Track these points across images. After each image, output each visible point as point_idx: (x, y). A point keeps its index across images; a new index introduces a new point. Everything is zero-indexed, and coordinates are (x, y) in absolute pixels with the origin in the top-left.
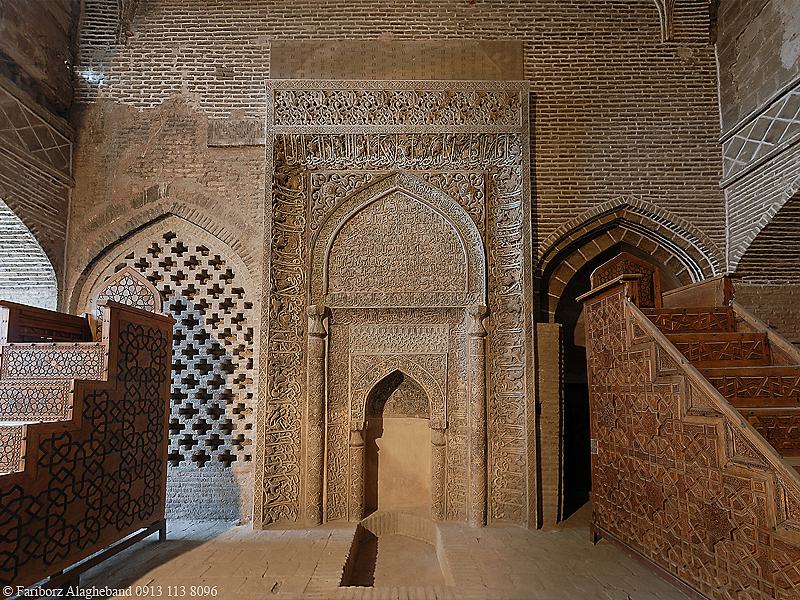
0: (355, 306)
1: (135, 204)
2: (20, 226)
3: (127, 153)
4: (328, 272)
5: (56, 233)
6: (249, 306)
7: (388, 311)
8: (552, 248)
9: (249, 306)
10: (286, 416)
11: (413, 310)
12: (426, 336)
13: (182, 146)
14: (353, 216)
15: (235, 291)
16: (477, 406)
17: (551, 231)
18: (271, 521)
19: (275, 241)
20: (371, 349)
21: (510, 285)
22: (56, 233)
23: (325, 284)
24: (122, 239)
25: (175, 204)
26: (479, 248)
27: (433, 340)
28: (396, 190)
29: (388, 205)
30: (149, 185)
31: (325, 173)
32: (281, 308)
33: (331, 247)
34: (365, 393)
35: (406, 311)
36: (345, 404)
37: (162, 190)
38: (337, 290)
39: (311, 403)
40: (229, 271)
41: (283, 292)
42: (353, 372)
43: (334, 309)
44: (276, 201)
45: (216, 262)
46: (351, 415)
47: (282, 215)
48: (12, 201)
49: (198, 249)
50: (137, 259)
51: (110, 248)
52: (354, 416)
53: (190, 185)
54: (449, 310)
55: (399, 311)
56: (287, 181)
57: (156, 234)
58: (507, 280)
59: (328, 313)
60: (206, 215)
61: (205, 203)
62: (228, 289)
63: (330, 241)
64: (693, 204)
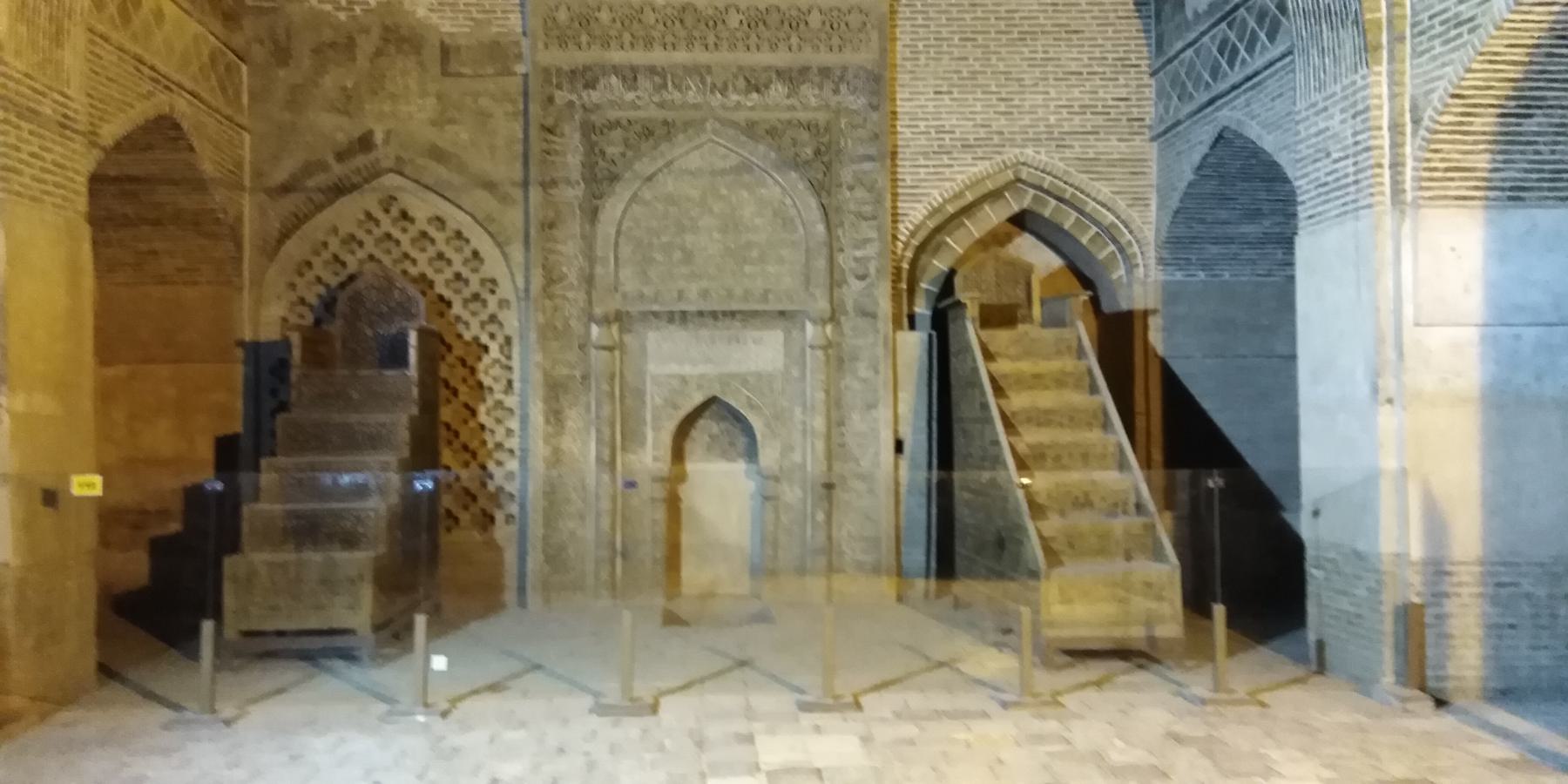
0: (656, 308)
3: (328, 81)
6: (504, 303)
7: (701, 314)
8: (918, 228)
9: (504, 303)
15: (483, 282)
16: (820, 445)
26: (821, 228)
27: (762, 352)
34: (670, 426)
35: (725, 314)
36: (643, 444)
37: (379, 137)
38: (630, 281)
39: (599, 441)
42: (654, 397)
46: (651, 456)
49: (430, 221)
52: (656, 459)
54: (782, 313)
55: (714, 315)
57: (368, 200)
62: (474, 280)
64: (1112, 163)
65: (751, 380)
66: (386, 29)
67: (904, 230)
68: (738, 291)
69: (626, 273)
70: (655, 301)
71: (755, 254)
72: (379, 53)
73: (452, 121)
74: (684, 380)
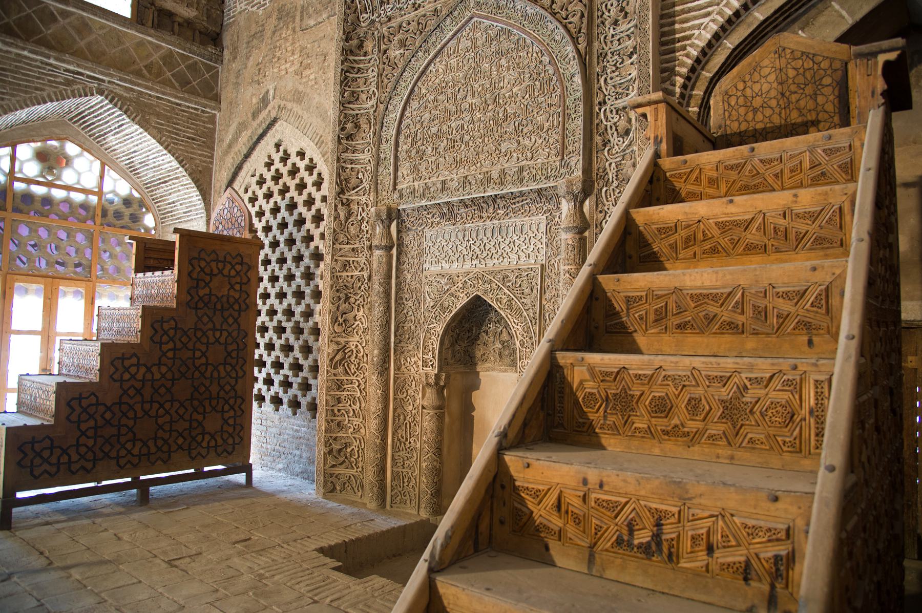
0: (423, 203)
1: (255, 115)
2: (175, 164)
4: (396, 158)
5: (204, 162)
10: (353, 358)
11: (494, 198)
12: (515, 238)
13: (286, 39)
14: (423, 72)
17: (708, 14)
18: (334, 489)
19: (343, 129)
20: (447, 265)
21: (627, 132)
22: (204, 162)
23: (392, 177)
24: (247, 156)
25: (279, 107)
28: (471, 18)
29: (465, 43)
30: (264, 91)
31: (394, 24)
32: (349, 214)
33: (400, 123)
37: (271, 92)
40: (320, 174)
41: (352, 195)
43: (404, 210)
44: (346, 78)
45: (310, 168)
47: (353, 92)
48: (165, 141)
50: (258, 174)
51: (239, 168)
53: (289, 83)
54: (539, 192)
56: (360, 46)
58: (622, 124)
59: (393, 215)
60: (300, 113)
61: (299, 97)
63: (398, 115)
65: (512, 277)
66: (280, 10)
67: (685, 60)
68: (495, 175)
69: (404, 170)
70: (423, 195)
71: (510, 129)
72: (274, 33)
73: (309, 66)
74: (451, 278)
